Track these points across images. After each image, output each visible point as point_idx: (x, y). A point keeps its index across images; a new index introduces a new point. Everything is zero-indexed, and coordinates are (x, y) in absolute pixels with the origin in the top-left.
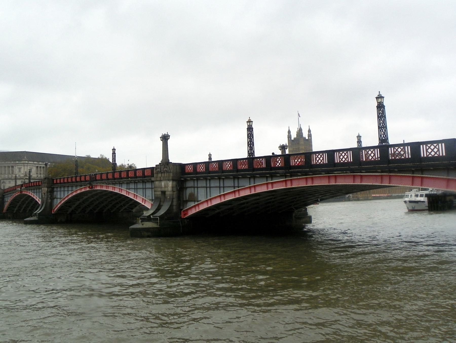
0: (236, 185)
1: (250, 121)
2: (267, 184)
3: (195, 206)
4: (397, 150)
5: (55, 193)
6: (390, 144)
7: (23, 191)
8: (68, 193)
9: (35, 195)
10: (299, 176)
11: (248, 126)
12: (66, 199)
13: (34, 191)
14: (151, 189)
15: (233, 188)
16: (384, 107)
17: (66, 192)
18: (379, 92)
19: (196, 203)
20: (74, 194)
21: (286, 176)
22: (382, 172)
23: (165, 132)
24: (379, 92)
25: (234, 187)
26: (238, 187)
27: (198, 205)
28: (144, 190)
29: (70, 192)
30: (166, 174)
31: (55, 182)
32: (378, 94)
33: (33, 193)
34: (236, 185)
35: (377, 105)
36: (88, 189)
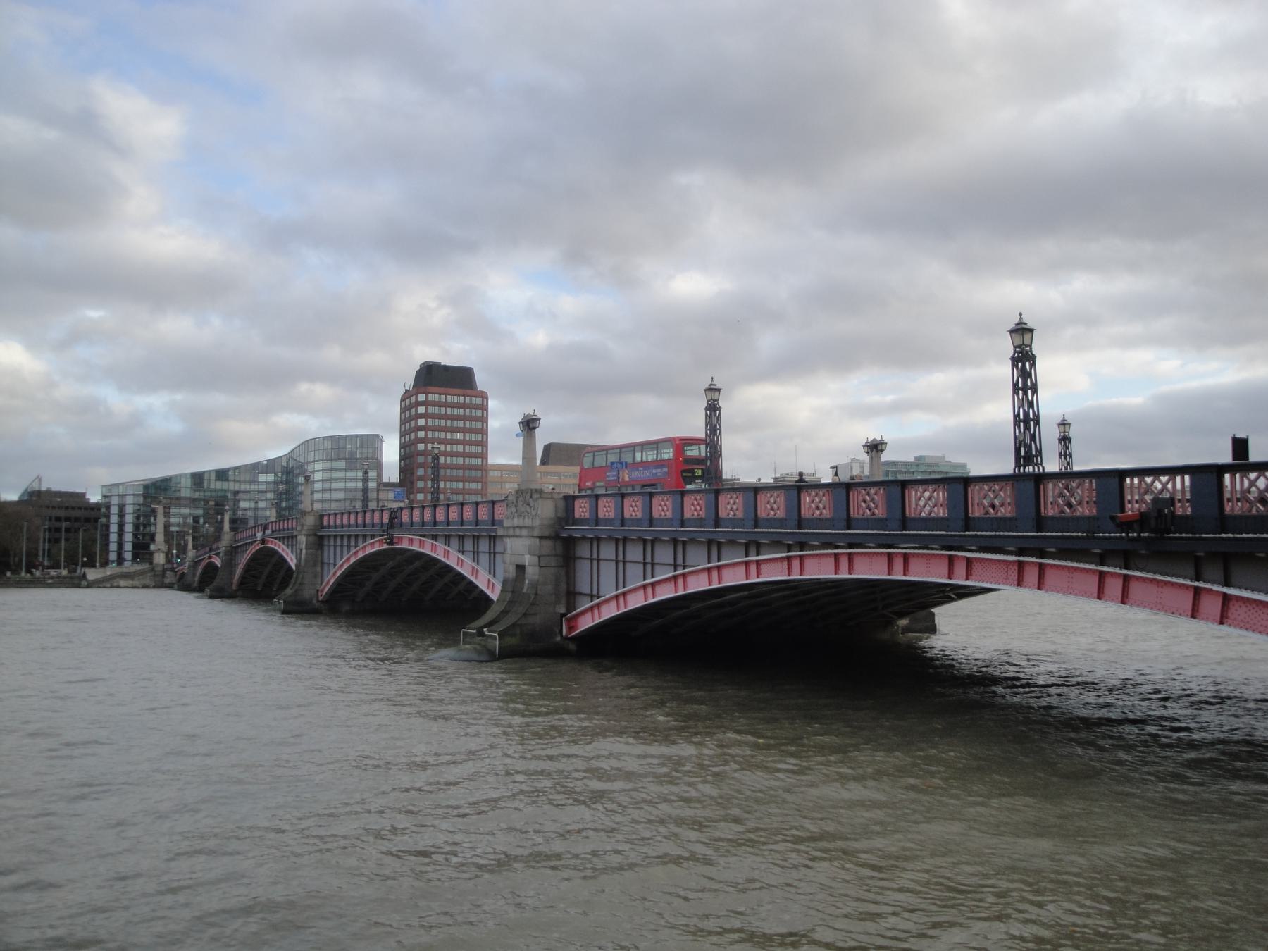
0: (680, 561)
1: (712, 390)
2: (747, 563)
3: (591, 609)
4: (1252, 483)
5: (326, 548)
6: (1046, 470)
7: (400, 539)
8: (348, 552)
9: (289, 551)
10: (816, 548)
11: (708, 401)
12: (345, 567)
13: (288, 542)
14: (488, 555)
15: (673, 568)
16: (1032, 359)
17: (345, 549)
18: (1021, 315)
19: (596, 601)
20: (360, 555)
21: (789, 548)
22: (1021, 552)
23: (529, 410)
24: (1021, 315)
25: (676, 568)
26: (684, 567)
27: (598, 605)
28: (595, 563)
29: (353, 551)
30: (526, 520)
31: (325, 523)
32: (1017, 321)
33: (285, 547)
34: (680, 561)
35: (1012, 353)
36: (385, 546)
